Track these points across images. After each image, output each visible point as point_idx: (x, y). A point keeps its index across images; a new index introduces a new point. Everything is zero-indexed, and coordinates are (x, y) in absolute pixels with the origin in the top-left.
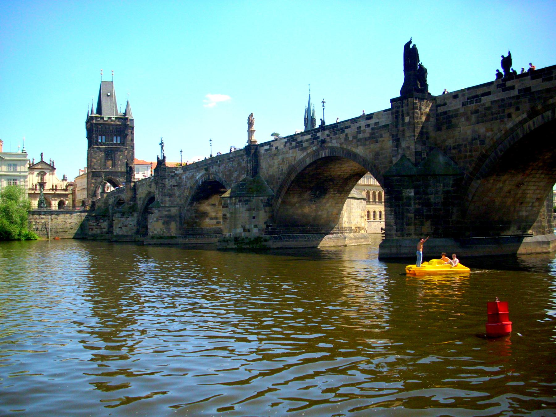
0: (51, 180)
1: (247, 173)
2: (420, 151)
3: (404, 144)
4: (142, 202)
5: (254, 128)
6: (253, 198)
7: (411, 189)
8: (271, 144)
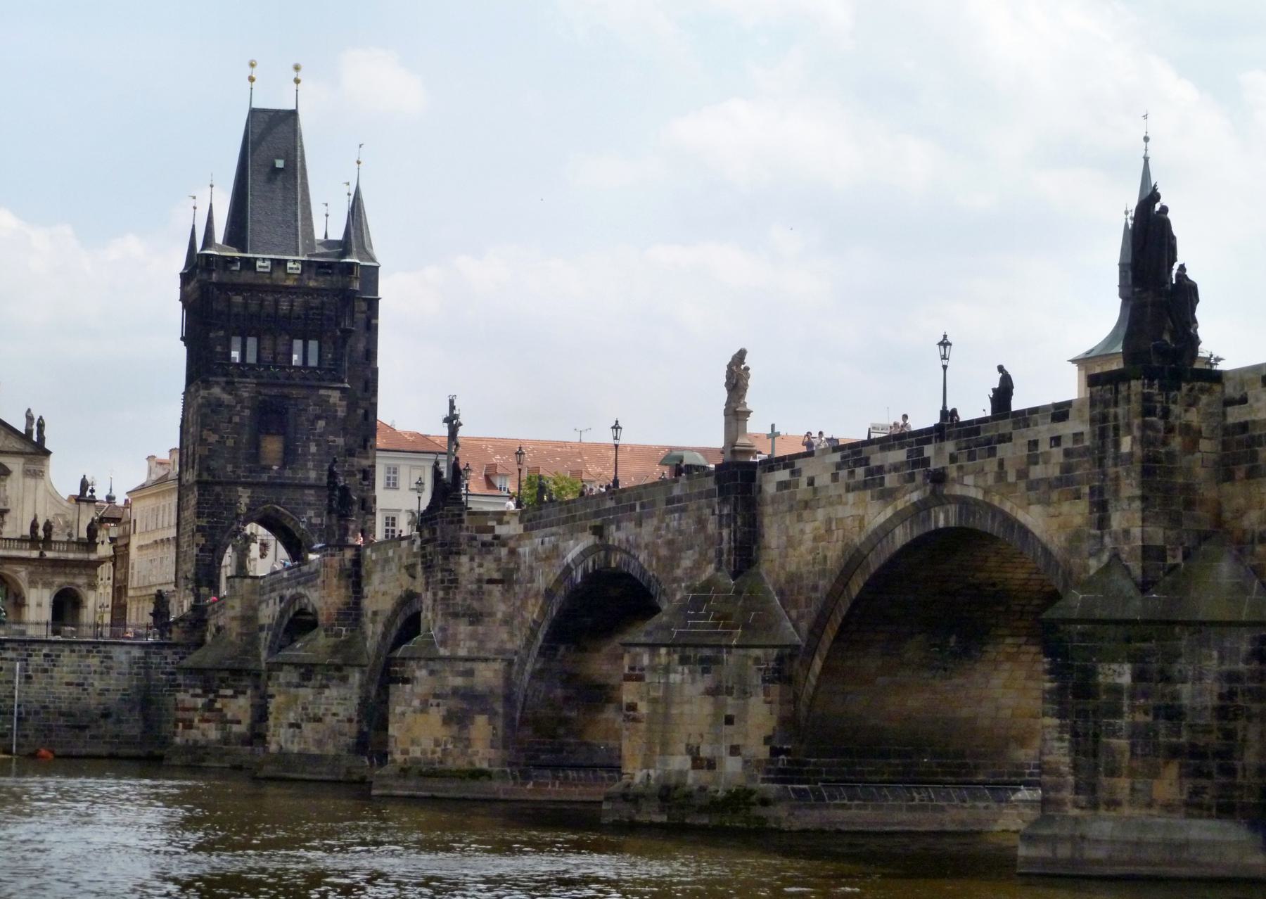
1: (720, 562)
2: (1162, 544)
3: (1117, 521)
4: (380, 628)
7: (1122, 662)
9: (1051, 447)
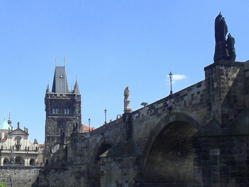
0: (25, 143)
2: (228, 113)
3: (214, 108)
5: (129, 99)
6: (124, 158)
7: (217, 149)
8: (140, 112)
9: (197, 95)
